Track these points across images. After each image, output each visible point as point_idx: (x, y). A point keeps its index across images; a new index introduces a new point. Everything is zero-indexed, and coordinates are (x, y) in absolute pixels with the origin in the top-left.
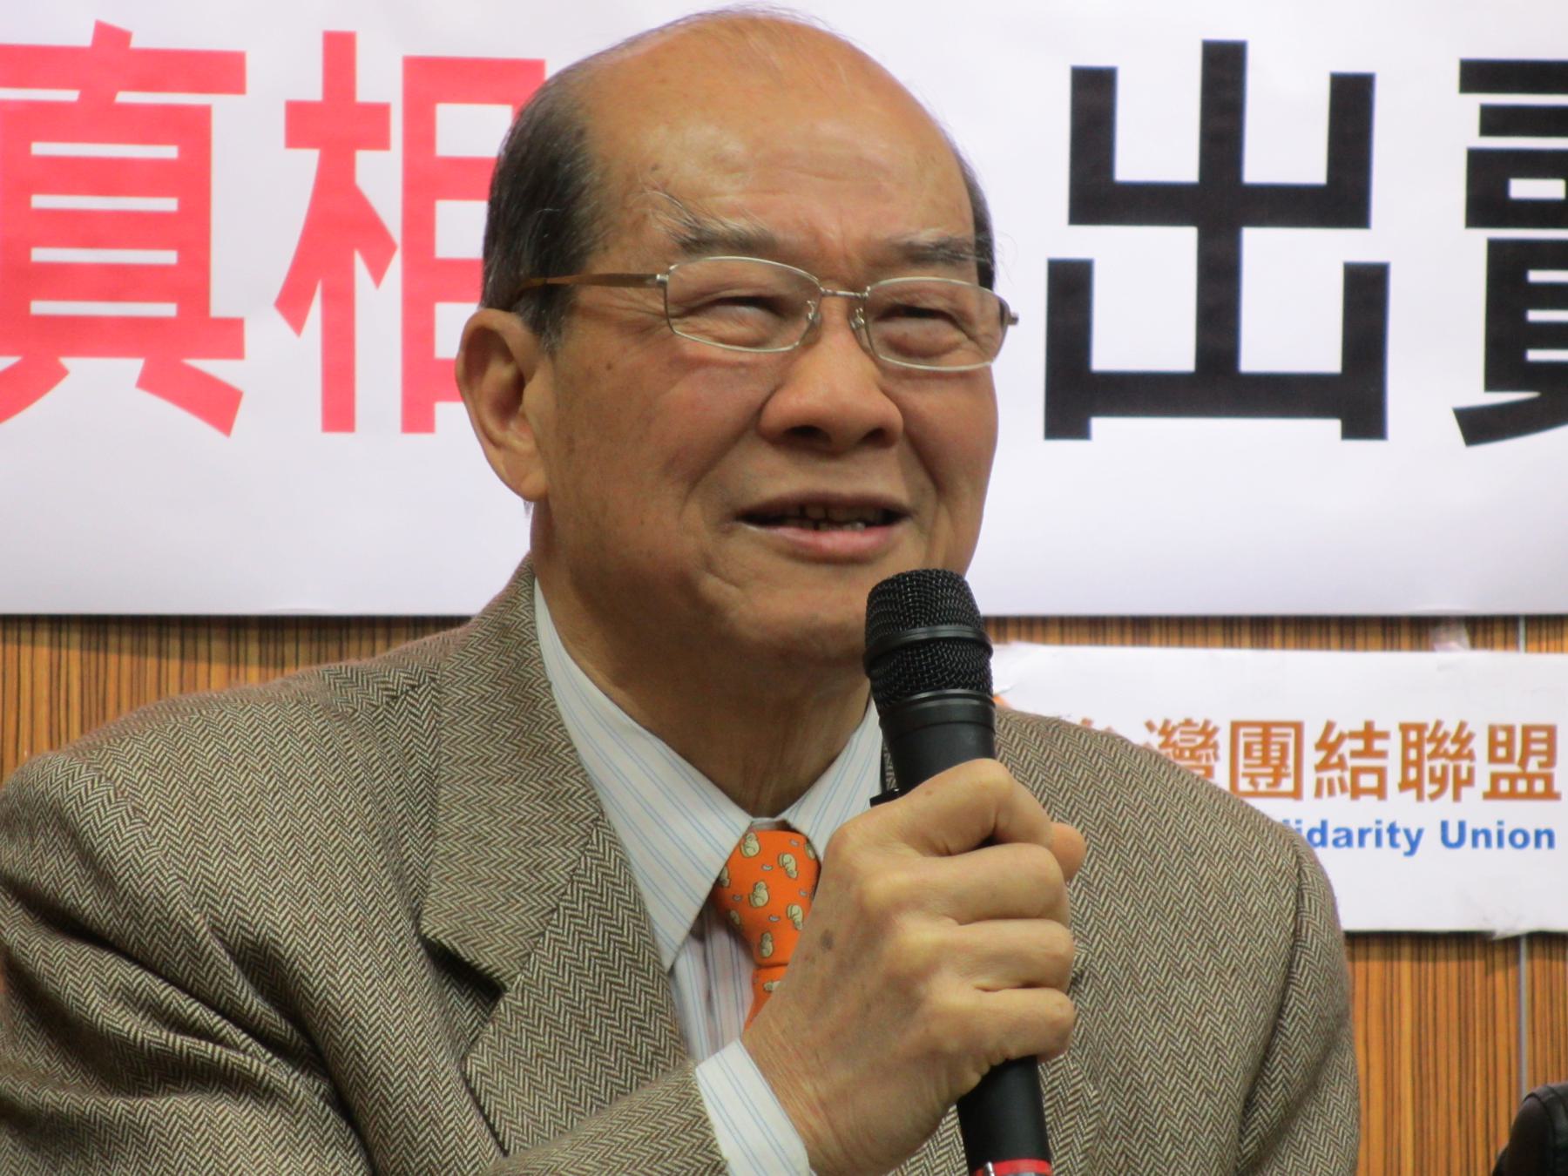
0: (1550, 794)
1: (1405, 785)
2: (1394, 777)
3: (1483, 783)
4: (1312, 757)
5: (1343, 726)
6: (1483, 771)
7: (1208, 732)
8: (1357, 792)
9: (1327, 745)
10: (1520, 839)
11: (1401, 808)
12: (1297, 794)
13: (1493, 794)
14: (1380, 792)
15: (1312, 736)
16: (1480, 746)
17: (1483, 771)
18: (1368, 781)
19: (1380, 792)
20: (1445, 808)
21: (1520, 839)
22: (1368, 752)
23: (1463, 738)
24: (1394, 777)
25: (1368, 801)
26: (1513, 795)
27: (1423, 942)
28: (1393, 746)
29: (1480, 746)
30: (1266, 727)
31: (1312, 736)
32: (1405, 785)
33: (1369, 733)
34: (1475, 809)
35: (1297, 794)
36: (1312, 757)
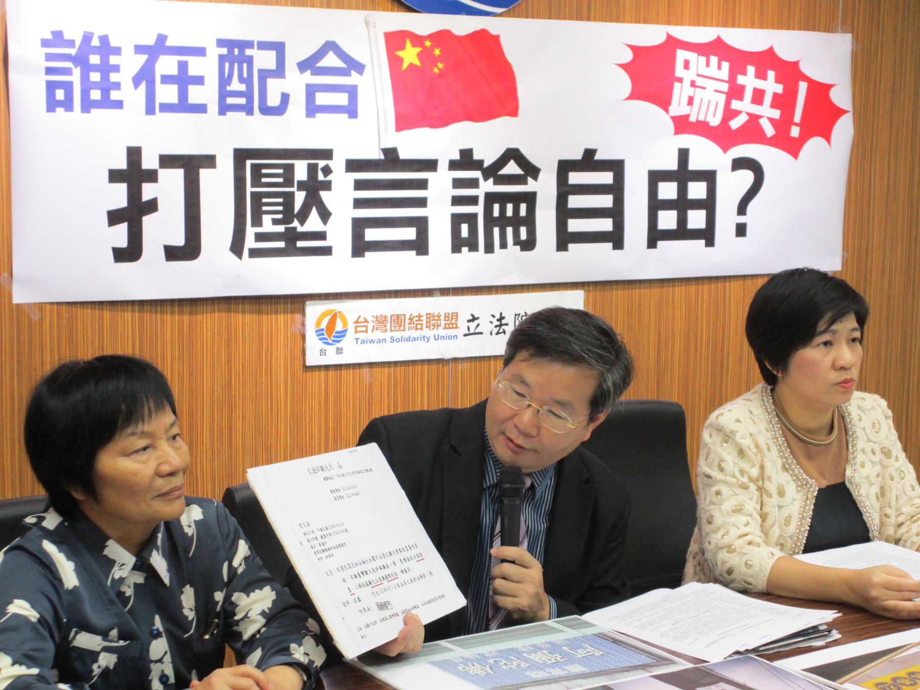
0: (457, 327)
1: (427, 327)
2: (424, 326)
3: (443, 326)
4: (407, 321)
5: (414, 315)
6: (443, 323)
7: (386, 317)
8: (417, 329)
9: (410, 319)
10: (450, 337)
11: (426, 332)
12: (404, 330)
13: (445, 328)
14: (421, 329)
15: (407, 317)
16: (442, 318)
17: (443, 323)
18: (419, 326)
19: (421, 329)
20: (435, 332)
21: (450, 337)
22: (419, 320)
23: (439, 316)
24: (424, 326)
25: (419, 331)
26: (449, 328)
27: (429, 361)
28: (424, 319)
29: (442, 318)
30: (398, 315)
31: (407, 317)
32: (427, 327)
33: (419, 316)
34: (441, 331)
35: (404, 330)
36: (407, 321)
